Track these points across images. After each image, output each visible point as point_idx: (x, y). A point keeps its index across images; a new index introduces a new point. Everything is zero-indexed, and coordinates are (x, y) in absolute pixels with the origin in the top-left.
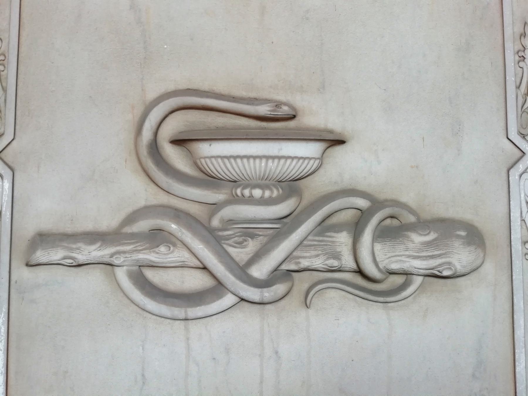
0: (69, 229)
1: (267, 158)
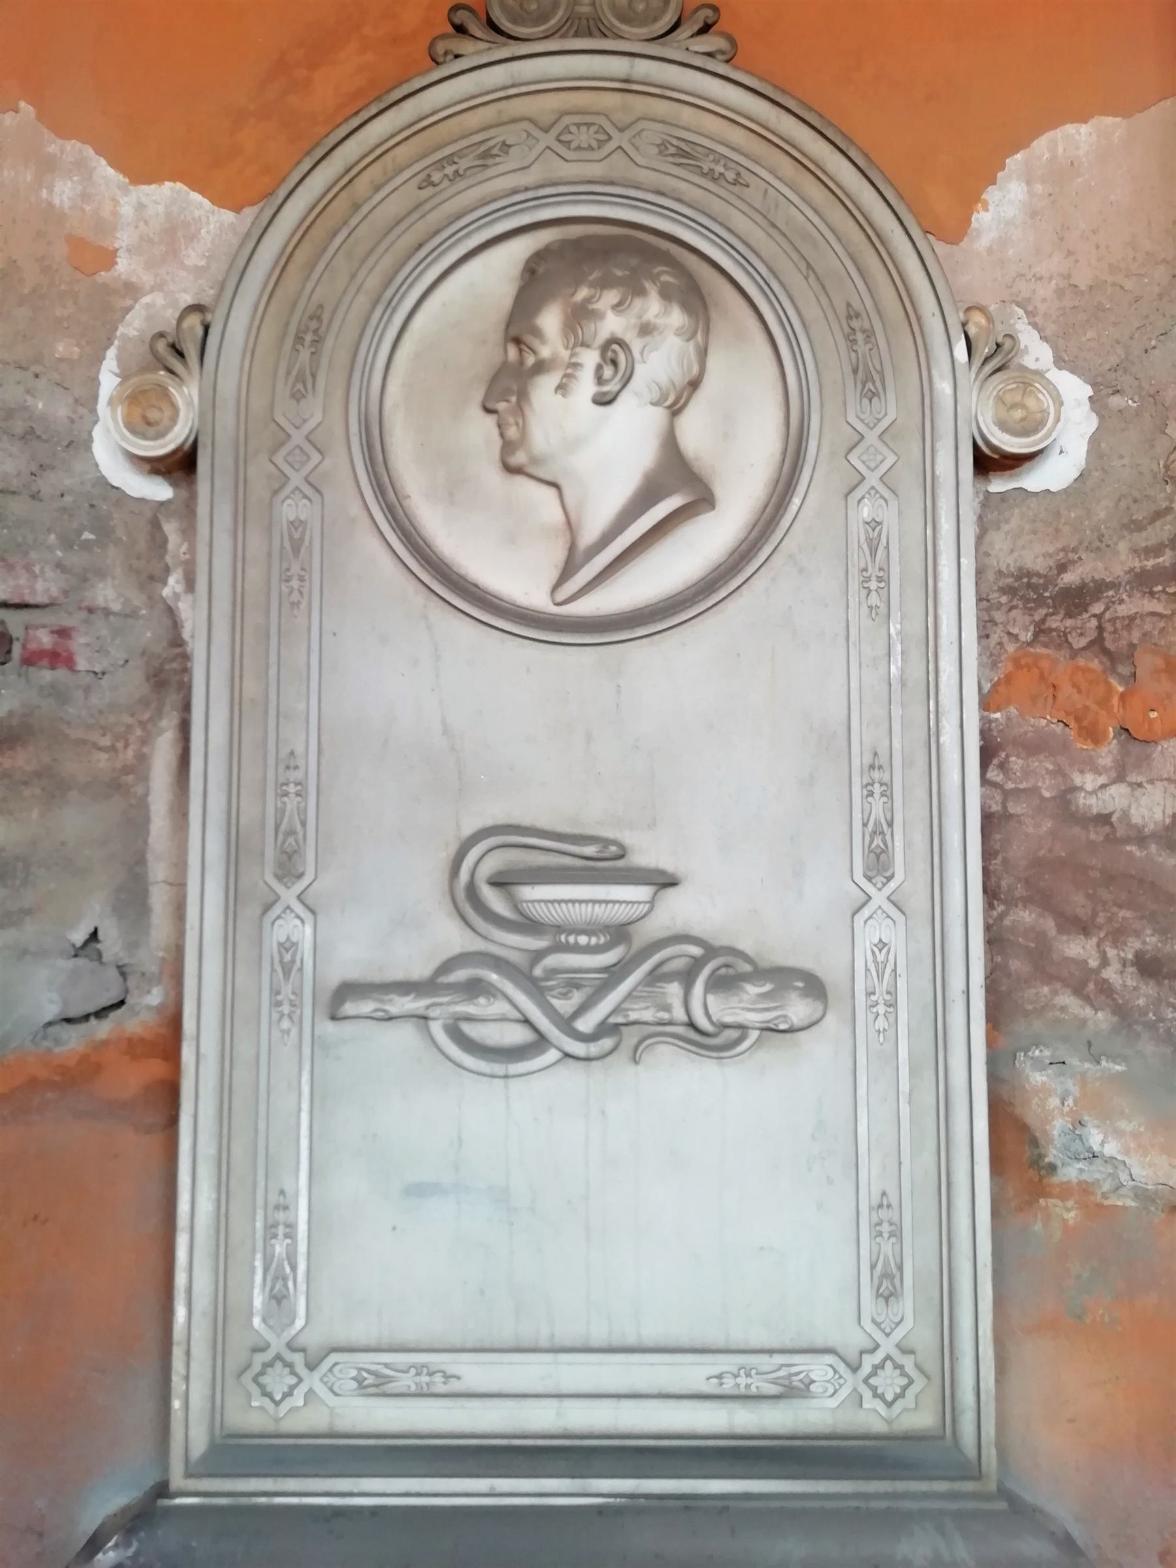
0: (377, 978)
1: (594, 902)
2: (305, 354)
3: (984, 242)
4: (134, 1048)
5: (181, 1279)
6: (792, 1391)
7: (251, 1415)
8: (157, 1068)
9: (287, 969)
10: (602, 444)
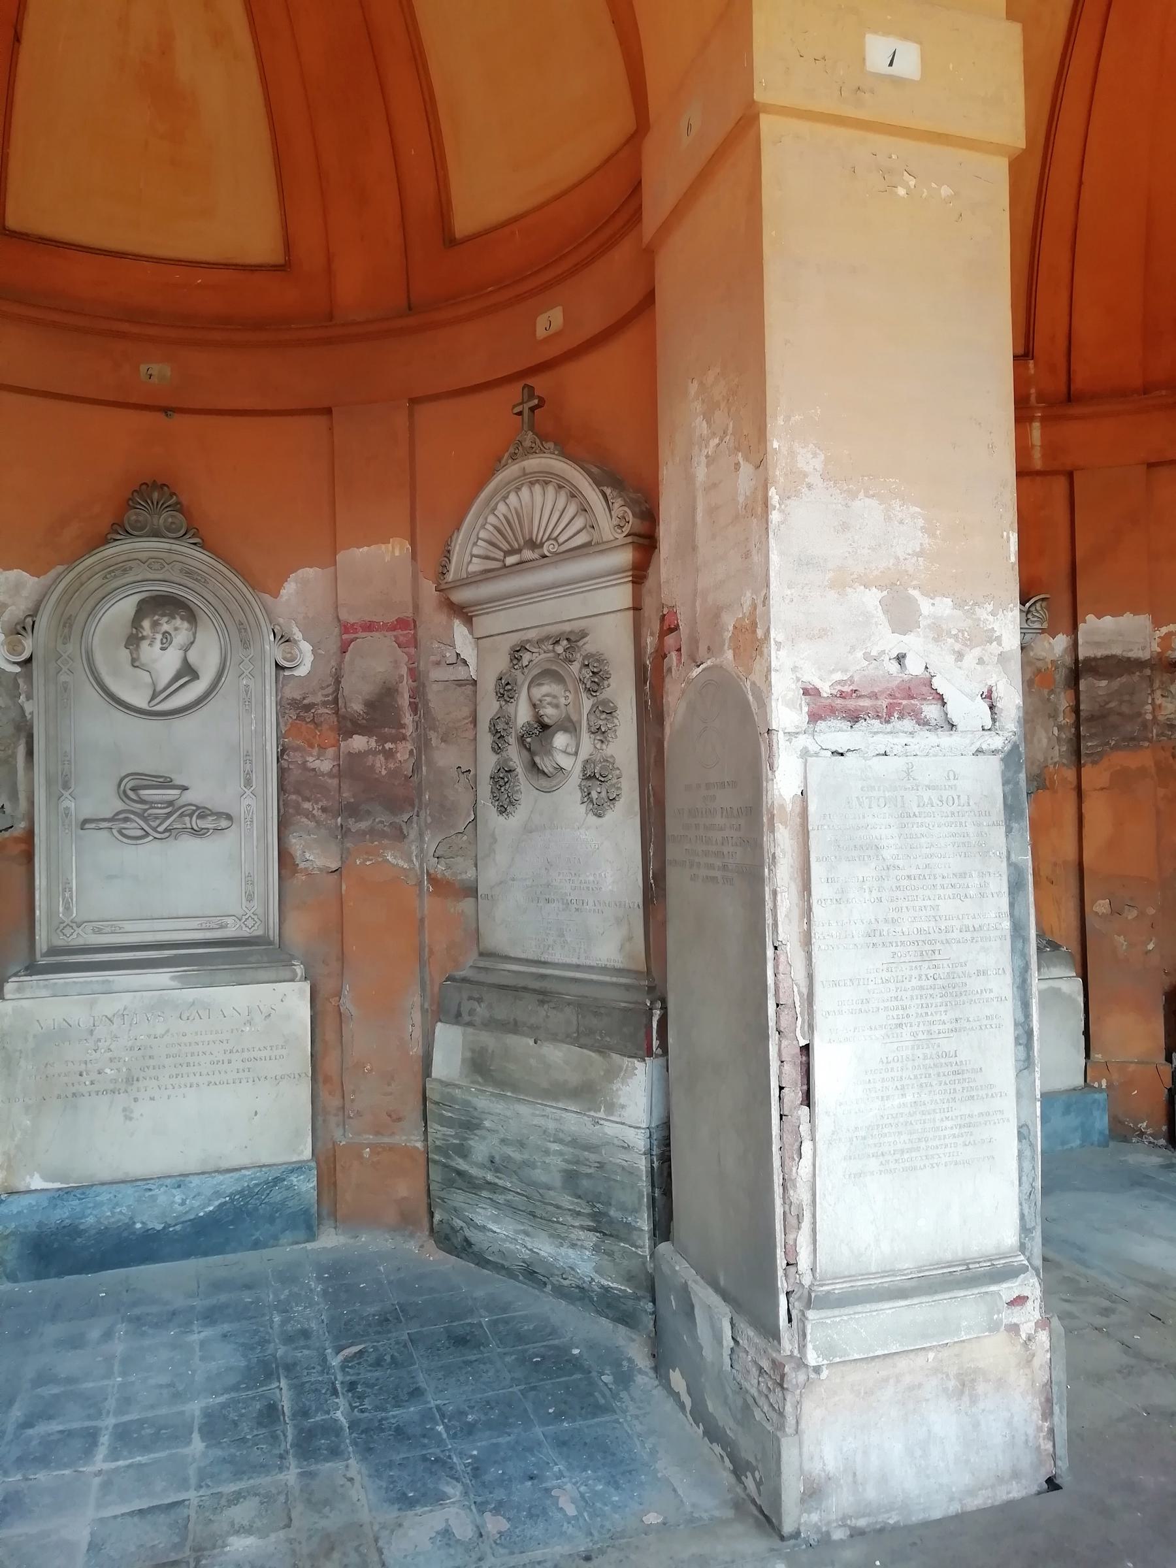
0: (95, 817)
2: (66, 630)
3: (284, 599)
4: (17, 840)
5: (37, 903)
6: (222, 927)
7: (60, 941)
8: (23, 846)
9: (67, 815)
10: (166, 662)
